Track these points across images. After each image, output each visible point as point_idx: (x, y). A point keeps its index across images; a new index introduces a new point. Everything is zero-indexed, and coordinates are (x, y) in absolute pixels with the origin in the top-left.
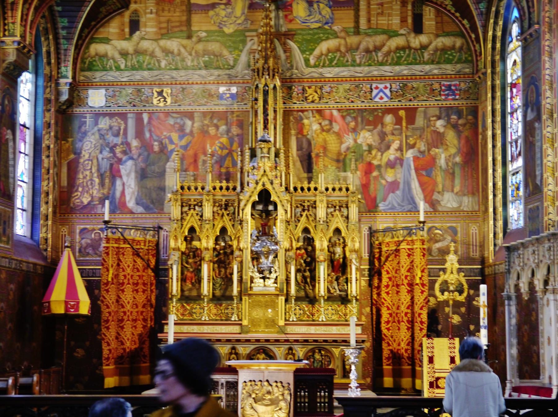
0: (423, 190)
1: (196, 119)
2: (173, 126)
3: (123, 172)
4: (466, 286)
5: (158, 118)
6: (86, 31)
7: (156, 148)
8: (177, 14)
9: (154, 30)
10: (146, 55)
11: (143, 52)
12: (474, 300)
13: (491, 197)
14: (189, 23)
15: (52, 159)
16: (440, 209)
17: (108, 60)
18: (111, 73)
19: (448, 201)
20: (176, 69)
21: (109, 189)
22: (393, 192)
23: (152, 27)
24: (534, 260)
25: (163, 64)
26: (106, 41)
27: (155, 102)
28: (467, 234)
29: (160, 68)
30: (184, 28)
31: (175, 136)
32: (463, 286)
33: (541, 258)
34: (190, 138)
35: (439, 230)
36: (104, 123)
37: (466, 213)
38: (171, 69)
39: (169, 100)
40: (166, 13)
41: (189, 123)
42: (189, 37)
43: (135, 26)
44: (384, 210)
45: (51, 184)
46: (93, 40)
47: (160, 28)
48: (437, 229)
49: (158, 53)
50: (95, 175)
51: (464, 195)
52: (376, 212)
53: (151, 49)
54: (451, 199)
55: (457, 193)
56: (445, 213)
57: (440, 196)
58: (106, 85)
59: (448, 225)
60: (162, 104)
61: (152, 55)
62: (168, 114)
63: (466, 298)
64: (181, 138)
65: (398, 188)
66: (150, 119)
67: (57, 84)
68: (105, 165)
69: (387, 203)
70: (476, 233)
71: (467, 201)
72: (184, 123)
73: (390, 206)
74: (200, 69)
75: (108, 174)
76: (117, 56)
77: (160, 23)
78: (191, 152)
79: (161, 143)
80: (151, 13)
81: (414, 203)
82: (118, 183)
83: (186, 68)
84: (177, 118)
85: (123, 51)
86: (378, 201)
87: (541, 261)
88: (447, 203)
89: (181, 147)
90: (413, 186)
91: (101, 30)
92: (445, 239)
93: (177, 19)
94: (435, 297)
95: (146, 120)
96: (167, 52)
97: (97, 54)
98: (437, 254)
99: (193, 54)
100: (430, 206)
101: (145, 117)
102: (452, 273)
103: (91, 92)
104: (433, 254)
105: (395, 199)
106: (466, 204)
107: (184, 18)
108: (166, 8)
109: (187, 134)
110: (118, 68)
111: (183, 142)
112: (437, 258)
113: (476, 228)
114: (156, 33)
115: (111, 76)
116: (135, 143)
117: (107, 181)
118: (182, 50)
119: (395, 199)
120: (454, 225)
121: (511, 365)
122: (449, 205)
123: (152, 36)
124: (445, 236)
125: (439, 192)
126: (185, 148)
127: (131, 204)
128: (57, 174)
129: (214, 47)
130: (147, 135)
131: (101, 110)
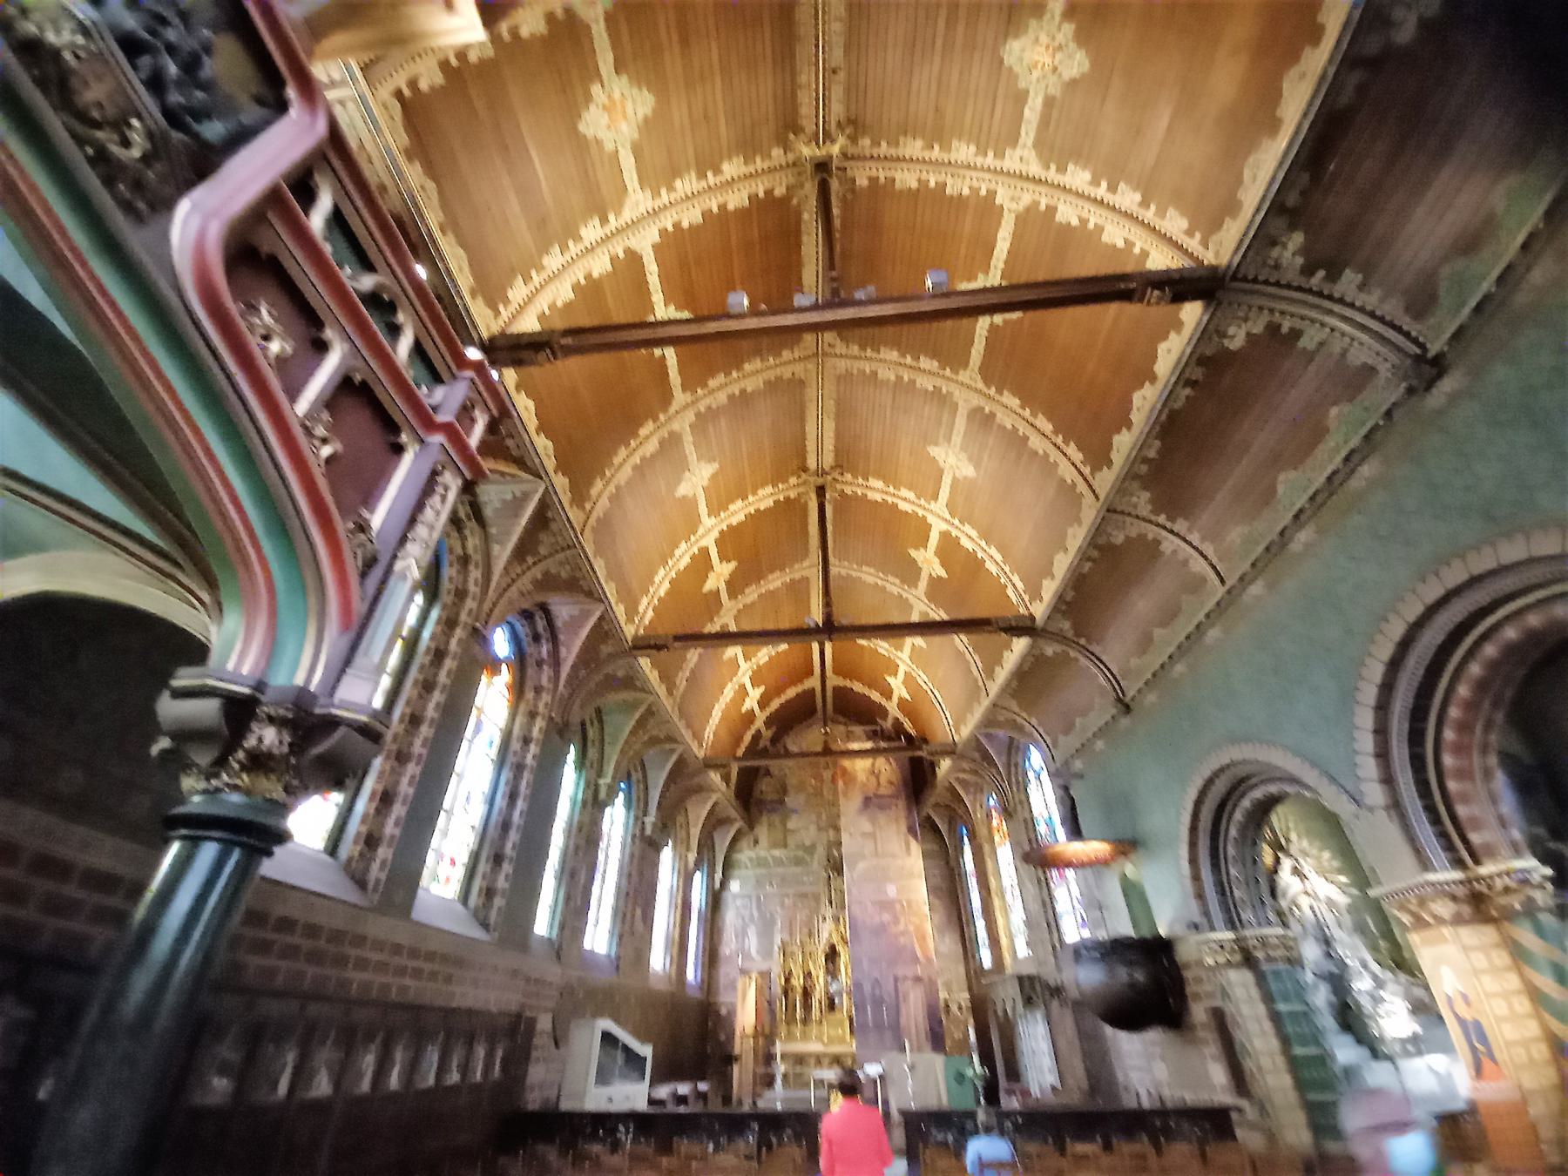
31: (779, 909)
36: (739, 902)
41: (786, 901)
42: (785, 846)
43: (756, 842)
49: (769, 858)
82: (747, 940)
96: (773, 857)
110: (747, 868)
116: (756, 914)
127: (753, 952)
129: (800, 853)
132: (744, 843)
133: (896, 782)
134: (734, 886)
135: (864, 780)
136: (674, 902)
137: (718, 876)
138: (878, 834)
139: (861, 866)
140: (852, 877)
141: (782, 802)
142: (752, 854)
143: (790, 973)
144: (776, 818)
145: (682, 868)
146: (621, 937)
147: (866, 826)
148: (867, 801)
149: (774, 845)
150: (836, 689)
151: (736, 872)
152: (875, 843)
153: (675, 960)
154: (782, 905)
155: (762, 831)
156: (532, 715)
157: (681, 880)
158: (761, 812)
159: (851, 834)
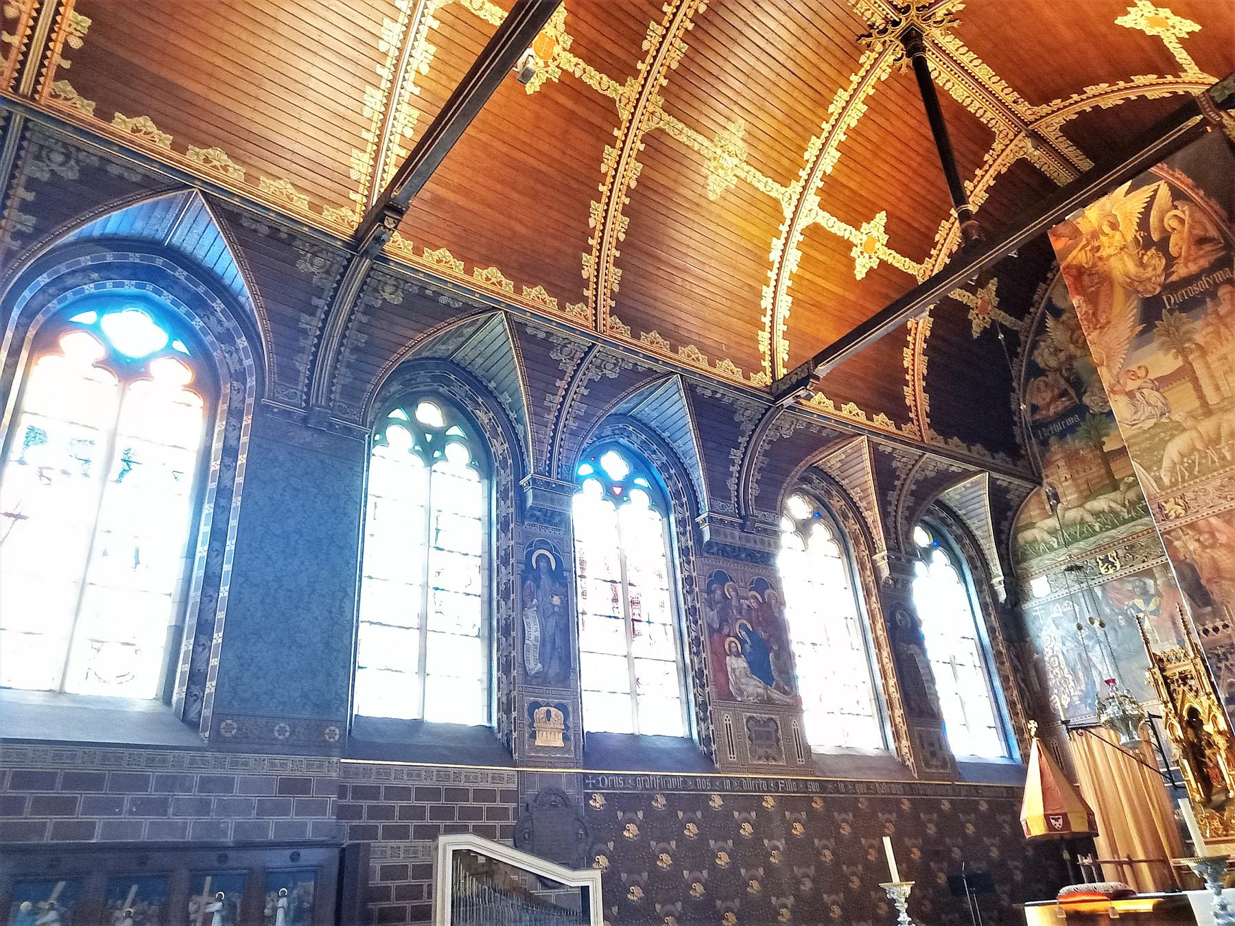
1: (1157, 576)
2: (1133, 592)
3: (1094, 659)
5: (1114, 588)
6: (1005, 525)
7: (1123, 623)
8: (1094, 470)
9: (1075, 496)
10: (1076, 524)
11: (1074, 524)
14: (1110, 474)
15: (1007, 664)
17: (1039, 544)
18: (1046, 556)
20: (1115, 527)
21: (1087, 684)
23: (1071, 494)
25: (1097, 529)
26: (1031, 525)
27: (1103, 571)
29: (1095, 533)
30: (1107, 482)
31: (1139, 603)
34: (1158, 599)
38: (1108, 530)
39: (1118, 564)
40: (1082, 474)
41: (1150, 582)
42: (1115, 488)
45: (1015, 693)
46: (1019, 530)
47: (1081, 492)
49: (1089, 518)
50: (1066, 671)
53: (1079, 517)
58: (1045, 571)
60: (1111, 571)
61: (1082, 522)
62: (1120, 580)
64: (1147, 602)
66: (1104, 590)
67: (991, 587)
68: (1073, 656)
72: (1145, 584)
74: (1141, 518)
75: (1079, 666)
76: (1046, 537)
77: (1077, 486)
78: (1166, 616)
79: (1125, 614)
80: (1066, 480)
83: (1125, 522)
84: (1134, 581)
85: (1051, 530)
89: (1152, 613)
91: (1022, 516)
93: (1096, 475)
95: (1099, 594)
96: (1097, 514)
97: (1026, 542)
99: (1127, 503)
101: (1098, 591)
103: (1032, 582)
107: (1103, 471)
108: (1080, 469)
109: (1153, 596)
111: (1152, 607)
114: (1078, 498)
115: (1047, 559)
117: (1081, 674)
118: (1113, 505)
123: (1076, 504)
126: (1155, 612)
128: (1024, 681)
130: (1107, 610)
131: (1048, 598)
132: (1032, 510)
133: (1213, 232)
134: (1039, 587)
135: (1131, 267)
136: (870, 637)
137: (998, 579)
138: (1198, 366)
139: (1173, 451)
140: (1158, 480)
141: (1081, 410)
142: (1052, 522)
143: (1193, 712)
144: (1074, 443)
145: (870, 579)
146: (702, 706)
147: (1164, 362)
148: (1151, 311)
149: (1091, 493)
150: (1068, 130)
151: (1034, 564)
152: (1198, 388)
153: (903, 728)
154: (1145, 594)
155: (1059, 477)
156: (235, 414)
157: (874, 599)
158: (1044, 443)
159: (1130, 395)
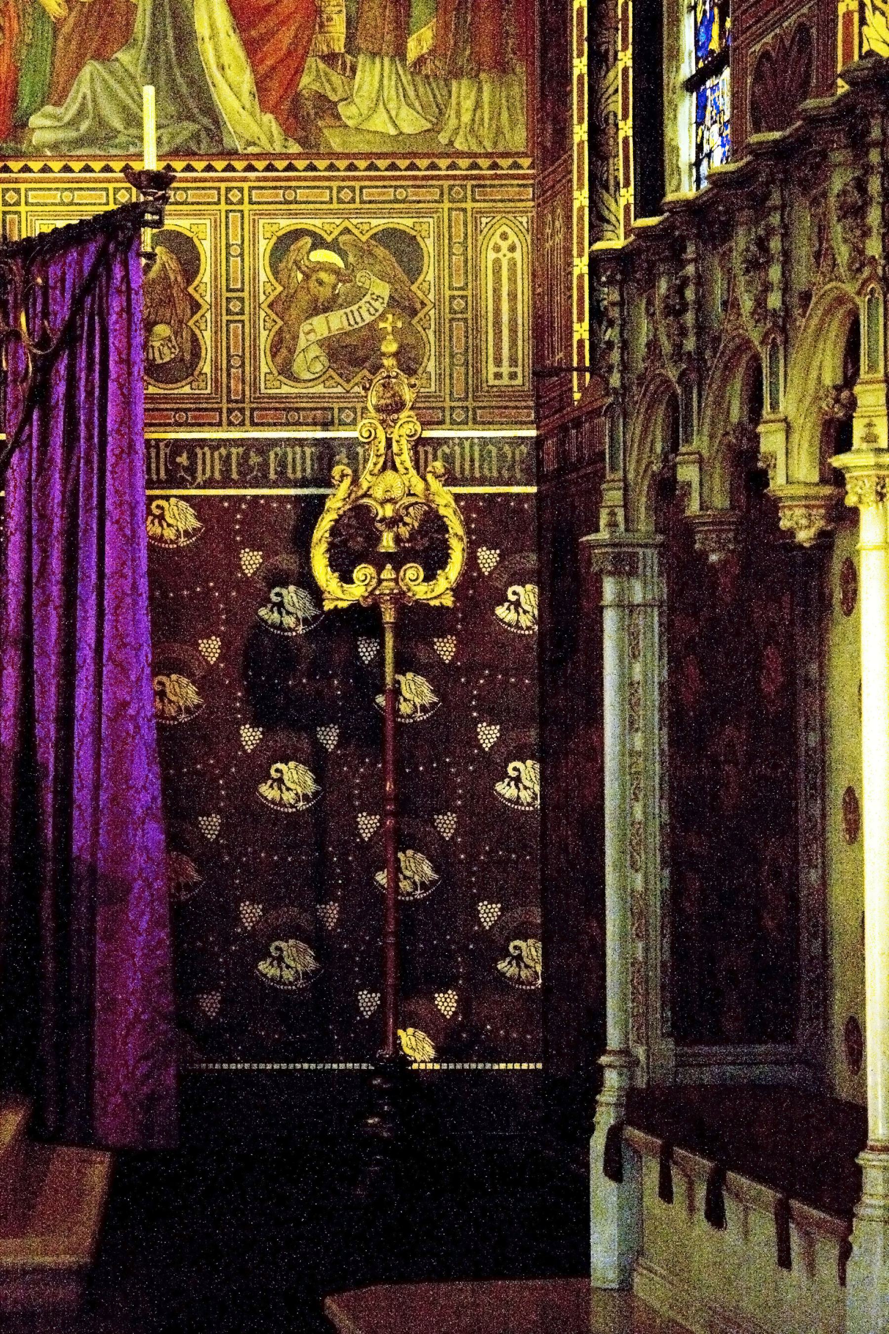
0: (252, 48)
4: (455, 525)
12: (502, 599)
13: (580, 66)
16: (335, 141)
19: (379, 99)
22: (100, 56)
24: (760, 302)
28: (472, 270)
32: (444, 529)
33: (802, 276)
35: (334, 246)
37: (464, 163)
44: (55, 146)
48: (319, 242)
51: (456, 74)
52: (18, 155)
54: (390, 91)
55: (420, 61)
56: (362, 164)
57: (336, 79)
59: (378, 224)
63: (458, 591)
65: (126, 38)
69: (70, 110)
70: (513, 264)
71: (468, 104)
73: (84, 126)
81: (210, 110)
86: (25, 102)
87: (806, 297)
88: (374, 110)
90: (202, 27)
92: (359, 294)
94: (307, 582)
98: (318, 367)
100: (288, 132)
102: (389, 465)
104: (299, 366)
105: (113, 95)
106: (466, 118)
112: (320, 389)
113: (512, 238)
119: (113, 95)
120: (405, 223)
121: (630, 964)
122: (380, 123)
124: (360, 277)
125: (330, 58)
